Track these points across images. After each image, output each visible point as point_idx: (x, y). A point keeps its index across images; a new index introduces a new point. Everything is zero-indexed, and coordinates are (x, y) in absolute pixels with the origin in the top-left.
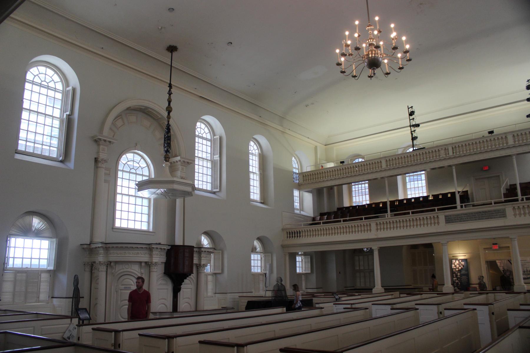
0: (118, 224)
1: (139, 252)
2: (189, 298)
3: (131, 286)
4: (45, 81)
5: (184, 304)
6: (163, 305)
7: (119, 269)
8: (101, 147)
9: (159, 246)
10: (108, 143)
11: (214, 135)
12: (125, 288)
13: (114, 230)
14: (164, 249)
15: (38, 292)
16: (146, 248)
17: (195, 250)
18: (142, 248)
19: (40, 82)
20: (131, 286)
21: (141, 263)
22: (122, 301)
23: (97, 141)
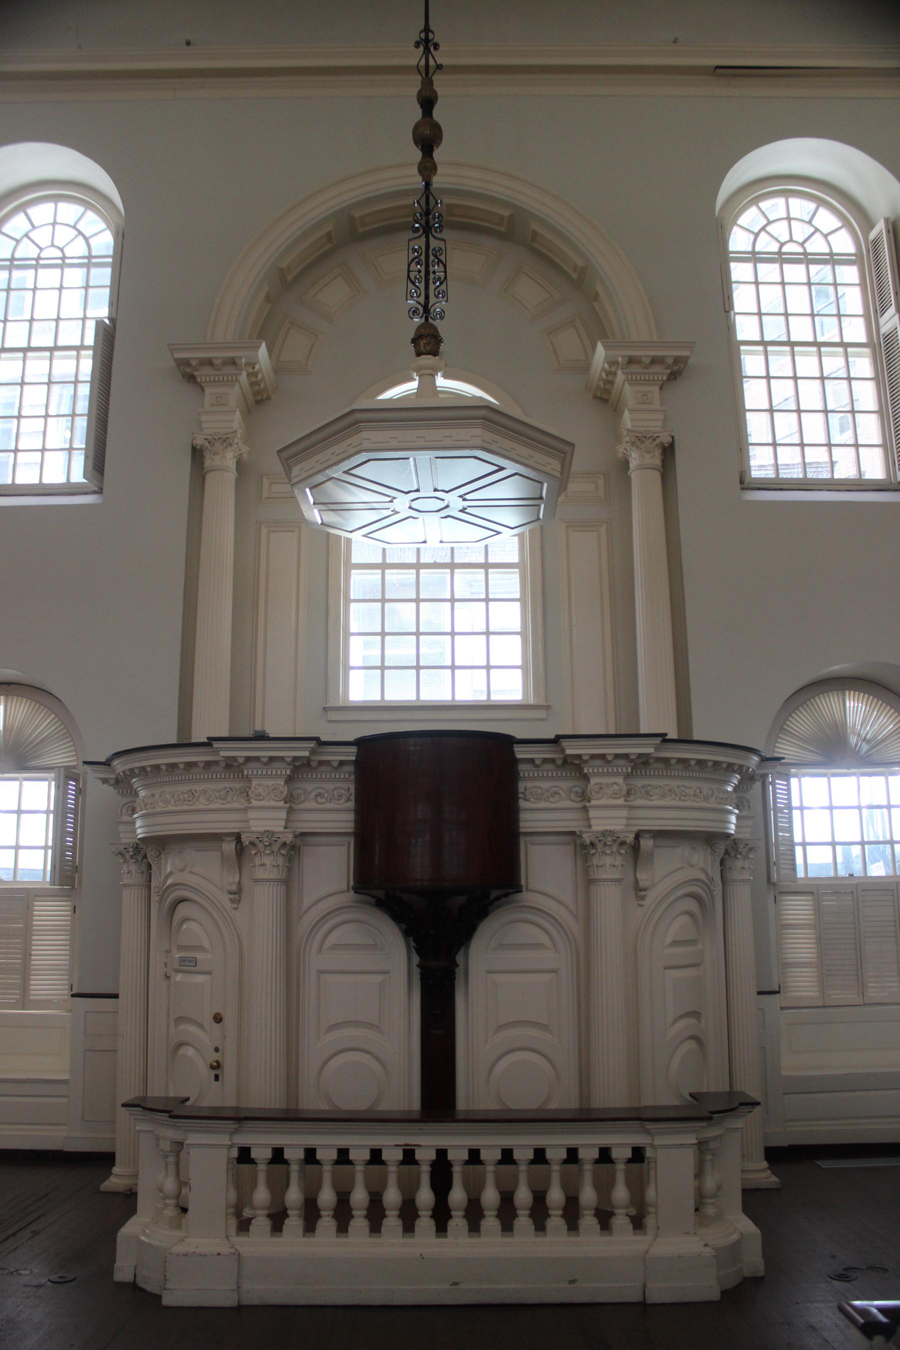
0: (361, 689)
1: (199, 787)
2: (544, 1027)
3: (199, 956)
4: (53, 245)
5: (499, 1058)
6: (358, 1056)
7: (169, 867)
8: (208, 391)
9: (263, 751)
10: (229, 370)
11: (867, 222)
12: (183, 960)
13: (333, 716)
14: (342, 763)
15: (25, 971)
16: (208, 764)
17: (521, 753)
18: (173, 766)
19: (33, 252)
20: (199, 956)
21: (217, 837)
22: (180, 1020)
23: (189, 374)
